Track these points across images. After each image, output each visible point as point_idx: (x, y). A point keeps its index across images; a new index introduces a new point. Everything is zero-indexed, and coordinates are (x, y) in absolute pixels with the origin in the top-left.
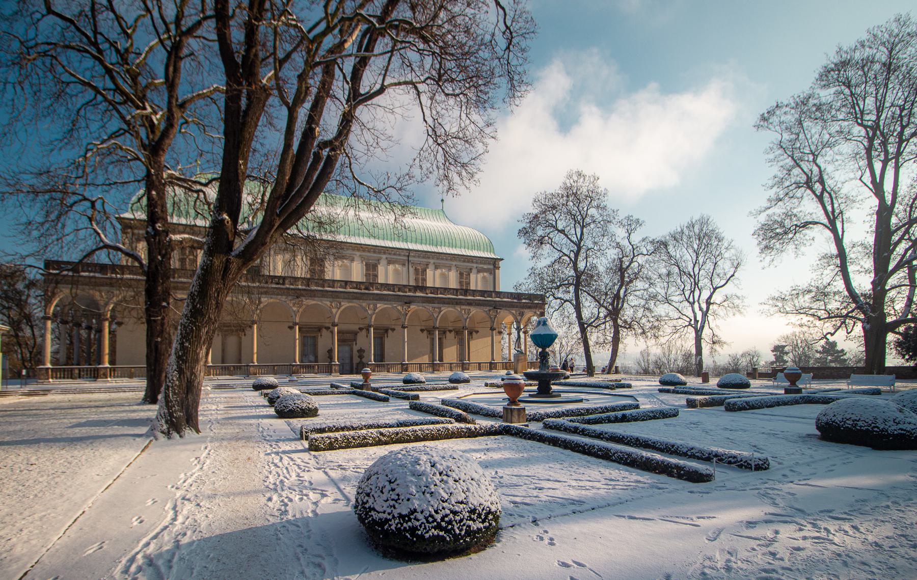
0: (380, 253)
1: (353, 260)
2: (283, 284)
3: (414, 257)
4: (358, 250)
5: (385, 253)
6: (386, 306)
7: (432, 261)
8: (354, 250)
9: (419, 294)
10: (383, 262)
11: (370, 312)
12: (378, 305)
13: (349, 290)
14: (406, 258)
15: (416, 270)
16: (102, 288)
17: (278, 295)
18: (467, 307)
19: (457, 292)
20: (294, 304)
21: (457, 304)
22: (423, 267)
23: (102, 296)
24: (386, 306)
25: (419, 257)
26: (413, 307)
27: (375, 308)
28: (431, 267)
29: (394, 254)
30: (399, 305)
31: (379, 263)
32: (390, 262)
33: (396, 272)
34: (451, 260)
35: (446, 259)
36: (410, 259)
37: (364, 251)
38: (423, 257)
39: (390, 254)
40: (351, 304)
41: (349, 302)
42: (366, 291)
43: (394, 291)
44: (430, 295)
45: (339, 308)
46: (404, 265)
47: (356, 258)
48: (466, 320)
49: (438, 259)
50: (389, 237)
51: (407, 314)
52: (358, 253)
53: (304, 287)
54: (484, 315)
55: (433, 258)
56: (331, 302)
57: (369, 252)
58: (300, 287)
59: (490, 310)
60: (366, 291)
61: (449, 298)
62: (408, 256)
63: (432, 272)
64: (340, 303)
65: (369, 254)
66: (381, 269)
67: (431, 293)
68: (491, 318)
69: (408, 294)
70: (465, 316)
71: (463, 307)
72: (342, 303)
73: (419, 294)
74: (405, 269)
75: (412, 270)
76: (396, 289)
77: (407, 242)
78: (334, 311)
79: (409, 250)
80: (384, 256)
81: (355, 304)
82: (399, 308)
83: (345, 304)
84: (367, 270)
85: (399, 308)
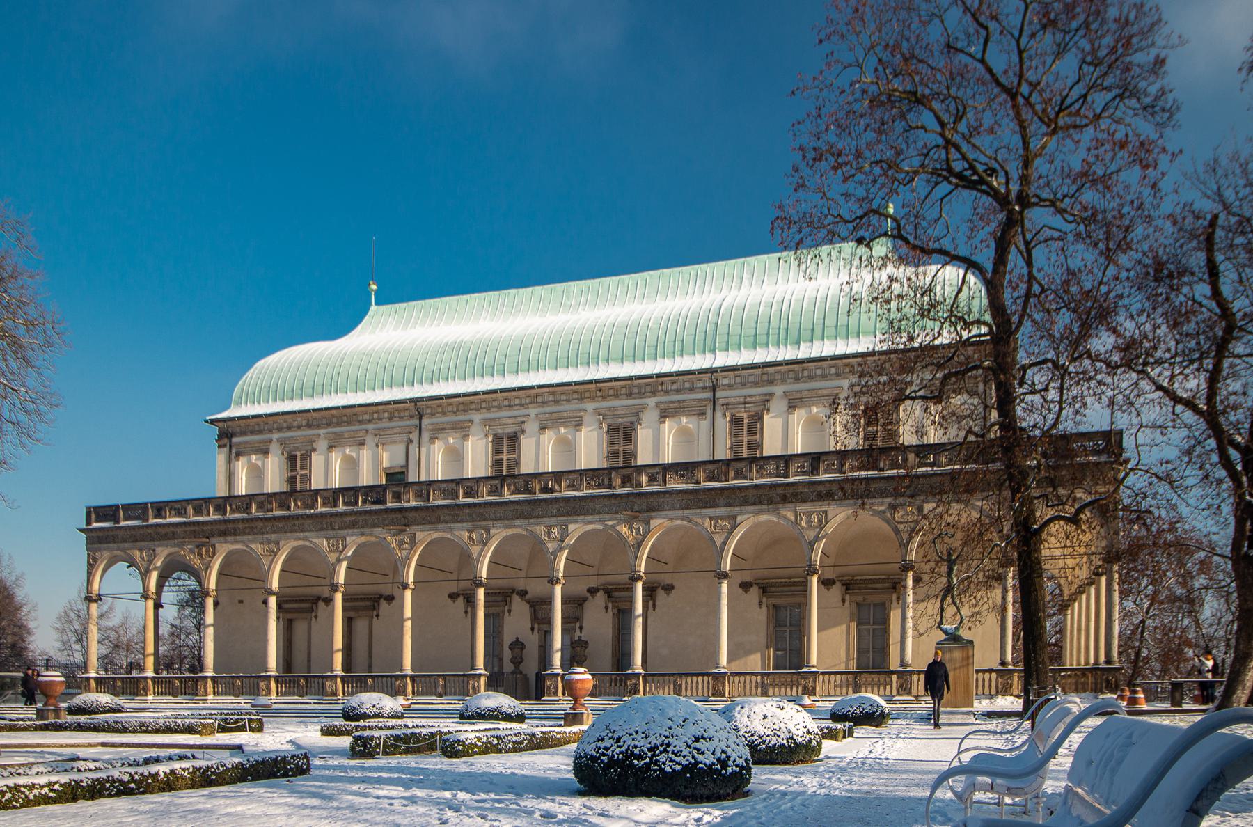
0: (642, 395)
1: (579, 425)
2: (384, 502)
3: (730, 386)
4: (592, 398)
5: (654, 393)
6: (589, 527)
7: (778, 390)
8: (581, 400)
9: (675, 484)
10: (650, 416)
11: (551, 546)
12: (571, 527)
13: (507, 496)
14: (708, 395)
15: (736, 423)
16: (143, 544)
17: (374, 526)
18: (818, 507)
19: (787, 467)
20: (401, 543)
21: (785, 500)
22: (753, 408)
23: (142, 558)
24: (589, 527)
25: (743, 385)
26: (659, 524)
27: (565, 534)
28: (778, 405)
29: (678, 391)
30: (621, 521)
31: (639, 421)
32: (665, 414)
33: (684, 434)
34: (838, 375)
35: (824, 377)
36: (718, 394)
37: (604, 398)
38: (756, 384)
39: (667, 392)
40: (510, 532)
41: (506, 527)
42: (544, 496)
43: (610, 486)
44: (705, 485)
45: (485, 544)
46: (702, 414)
47: (587, 419)
48: (812, 544)
49: (797, 380)
50: (669, 347)
51: (639, 545)
52: (590, 406)
53: (422, 504)
54: (878, 523)
55: (783, 381)
56: (470, 531)
57: (616, 396)
58: (413, 503)
59: (894, 508)
60: (544, 496)
61: (756, 487)
62: (714, 389)
63: (779, 421)
64: (488, 532)
65: (616, 403)
66: (643, 436)
67: (709, 479)
68: (897, 532)
69: (646, 488)
70: (810, 535)
71: (803, 508)
72: (493, 531)
73: (675, 484)
74: (705, 424)
75: (723, 424)
76: (617, 481)
77: (713, 351)
78: (475, 550)
79: (712, 371)
80: (651, 402)
81: (519, 529)
82: (623, 529)
83: (499, 534)
84: (612, 442)
85: (623, 529)
